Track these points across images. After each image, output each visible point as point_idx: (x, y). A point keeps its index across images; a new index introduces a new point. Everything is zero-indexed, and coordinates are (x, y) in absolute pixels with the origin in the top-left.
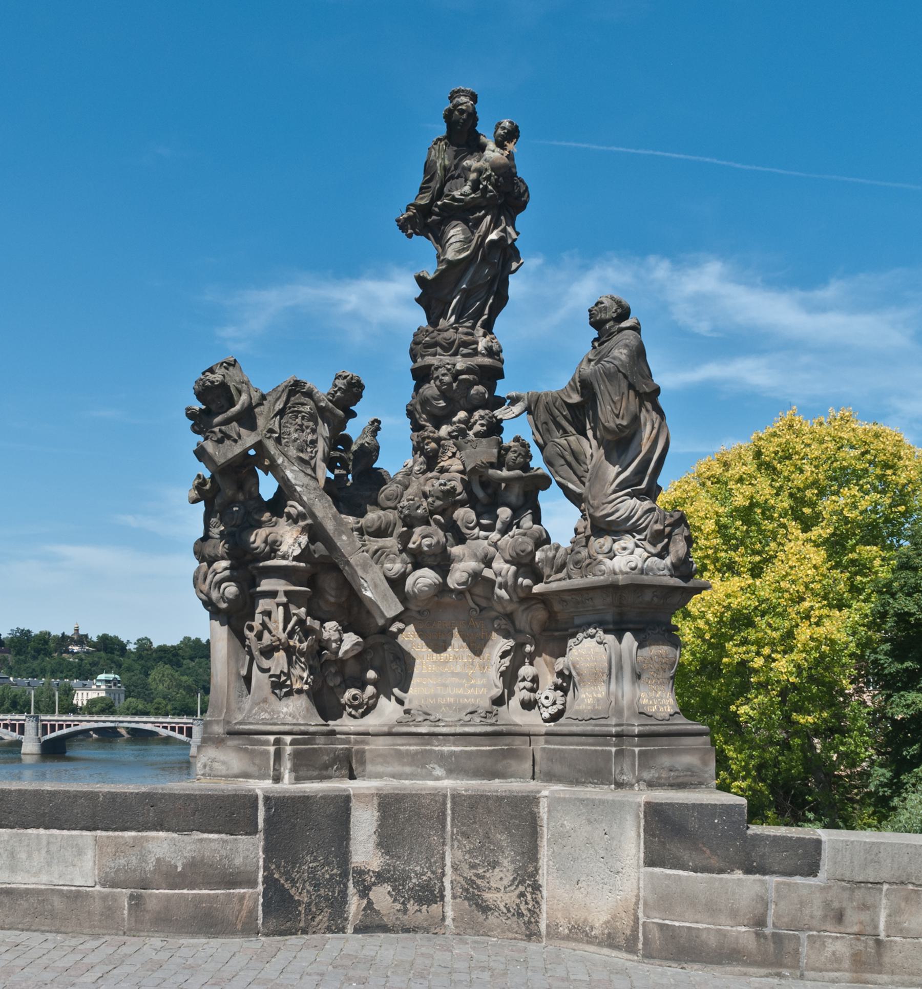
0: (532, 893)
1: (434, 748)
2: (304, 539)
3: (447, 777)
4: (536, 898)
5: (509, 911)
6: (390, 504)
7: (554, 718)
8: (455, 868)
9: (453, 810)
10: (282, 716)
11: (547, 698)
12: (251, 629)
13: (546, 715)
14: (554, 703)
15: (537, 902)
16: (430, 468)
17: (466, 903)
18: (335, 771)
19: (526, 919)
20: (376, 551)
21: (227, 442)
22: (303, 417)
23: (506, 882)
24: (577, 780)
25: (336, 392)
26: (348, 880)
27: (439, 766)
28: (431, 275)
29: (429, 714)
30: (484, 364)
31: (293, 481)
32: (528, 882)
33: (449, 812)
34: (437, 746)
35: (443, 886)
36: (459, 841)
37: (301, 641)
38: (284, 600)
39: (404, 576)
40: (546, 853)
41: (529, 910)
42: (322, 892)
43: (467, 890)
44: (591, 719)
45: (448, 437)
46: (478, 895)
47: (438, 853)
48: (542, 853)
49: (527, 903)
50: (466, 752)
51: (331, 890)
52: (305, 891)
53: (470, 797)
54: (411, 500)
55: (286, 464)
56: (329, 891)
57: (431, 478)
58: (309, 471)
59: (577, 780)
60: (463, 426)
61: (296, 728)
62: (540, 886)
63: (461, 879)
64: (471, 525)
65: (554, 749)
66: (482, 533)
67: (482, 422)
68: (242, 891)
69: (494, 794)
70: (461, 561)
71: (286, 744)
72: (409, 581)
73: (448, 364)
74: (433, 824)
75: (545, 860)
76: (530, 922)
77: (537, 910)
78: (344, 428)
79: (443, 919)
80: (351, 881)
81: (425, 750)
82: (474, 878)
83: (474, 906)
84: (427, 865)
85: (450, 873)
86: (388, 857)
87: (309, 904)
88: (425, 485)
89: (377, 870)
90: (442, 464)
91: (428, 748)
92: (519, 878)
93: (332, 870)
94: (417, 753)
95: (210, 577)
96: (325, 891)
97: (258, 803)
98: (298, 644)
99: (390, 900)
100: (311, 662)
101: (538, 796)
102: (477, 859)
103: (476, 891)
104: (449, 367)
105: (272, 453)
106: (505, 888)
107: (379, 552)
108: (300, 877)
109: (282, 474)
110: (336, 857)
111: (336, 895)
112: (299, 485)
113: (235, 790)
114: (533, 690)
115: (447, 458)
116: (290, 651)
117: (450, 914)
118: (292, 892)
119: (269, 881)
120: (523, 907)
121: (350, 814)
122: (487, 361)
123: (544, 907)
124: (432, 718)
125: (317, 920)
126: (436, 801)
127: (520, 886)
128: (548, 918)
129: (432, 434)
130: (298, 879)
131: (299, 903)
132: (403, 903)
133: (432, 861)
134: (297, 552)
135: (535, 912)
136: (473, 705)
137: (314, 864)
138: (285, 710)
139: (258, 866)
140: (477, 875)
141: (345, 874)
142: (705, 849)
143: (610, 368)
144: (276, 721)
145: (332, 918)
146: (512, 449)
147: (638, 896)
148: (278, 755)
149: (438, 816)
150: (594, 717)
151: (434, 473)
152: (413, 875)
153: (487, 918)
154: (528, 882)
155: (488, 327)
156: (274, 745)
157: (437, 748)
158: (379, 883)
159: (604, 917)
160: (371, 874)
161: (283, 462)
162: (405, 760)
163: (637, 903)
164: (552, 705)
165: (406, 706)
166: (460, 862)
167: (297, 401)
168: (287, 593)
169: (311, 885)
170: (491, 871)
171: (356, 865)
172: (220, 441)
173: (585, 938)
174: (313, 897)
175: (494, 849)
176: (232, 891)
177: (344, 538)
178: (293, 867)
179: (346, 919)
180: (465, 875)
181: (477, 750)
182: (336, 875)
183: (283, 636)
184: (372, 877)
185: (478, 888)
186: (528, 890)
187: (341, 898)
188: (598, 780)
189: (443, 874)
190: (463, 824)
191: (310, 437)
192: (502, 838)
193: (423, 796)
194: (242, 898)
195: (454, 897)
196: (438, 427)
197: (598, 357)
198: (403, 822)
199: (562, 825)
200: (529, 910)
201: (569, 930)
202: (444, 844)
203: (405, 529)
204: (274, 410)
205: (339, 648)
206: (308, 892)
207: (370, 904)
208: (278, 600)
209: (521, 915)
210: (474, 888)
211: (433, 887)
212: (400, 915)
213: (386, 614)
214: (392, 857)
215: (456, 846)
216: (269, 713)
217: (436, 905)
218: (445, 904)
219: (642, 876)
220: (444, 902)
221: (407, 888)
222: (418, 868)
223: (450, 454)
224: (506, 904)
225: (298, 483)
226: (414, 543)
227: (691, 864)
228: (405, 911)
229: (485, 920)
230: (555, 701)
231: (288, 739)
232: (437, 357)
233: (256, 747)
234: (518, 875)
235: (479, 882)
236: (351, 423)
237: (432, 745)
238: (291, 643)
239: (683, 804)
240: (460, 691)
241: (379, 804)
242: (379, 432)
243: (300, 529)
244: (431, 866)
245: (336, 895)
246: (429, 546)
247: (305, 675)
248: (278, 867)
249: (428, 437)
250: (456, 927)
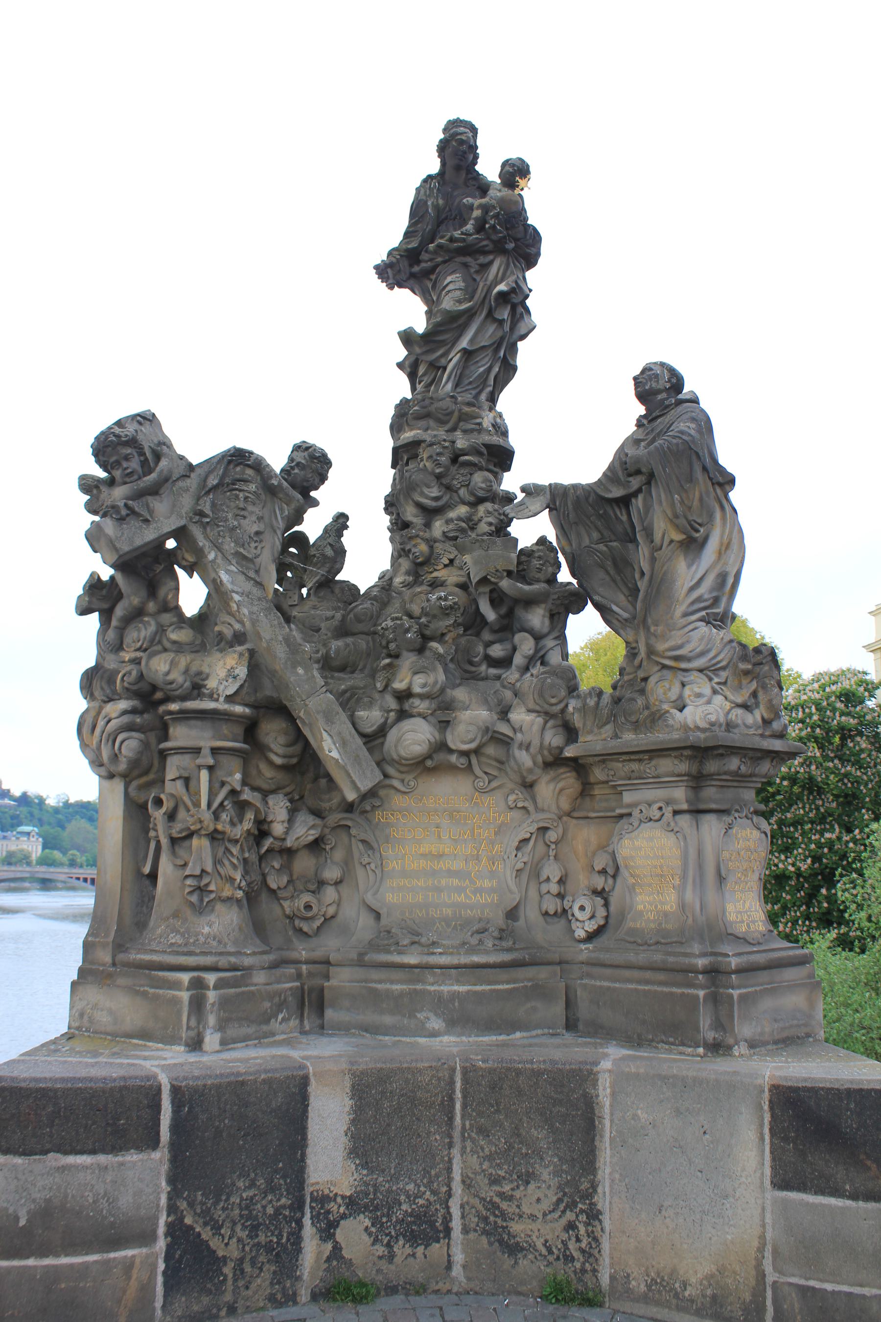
0: (587, 1224)
1: (428, 987)
2: (242, 672)
3: (447, 1032)
4: (593, 1232)
5: (550, 1252)
6: (360, 627)
7: (591, 937)
8: (467, 1183)
9: (465, 1092)
10: (202, 939)
11: (582, 908)
12: (159, 802)
13: (580, 933)
14: (592, 917)
15: (596, 1239)
16: (417, 581)
17: (484, 1238)
18: (280, 1023)
19: (578, 1265)
20: (345, 692)
21: (134, 523)
22: (246, 498)
23: (546, 1205)
24: (639, 1036)
25: (292, 468)
26: (303, 1216)
27: (436, 1014)
28: (421, 327)
29: (418, 934)
30: (493, 443)
31: (230, 586)
32: (580, 1205)
33: (458, 1095)
34: (432, 984)
35: (449, 1213)
36: (473, 1141)
37: (233, 824)
38: (211, 761)
39: (382, 731)
40: (608, 1160)
41: (583, 1251)
42: (262, 1238)
43: (485, 1219)
44: (658, 943)
45: (443, 539)
46: (502, 1227)
47: (442, 1160)
48: (602, 1160)
49: (578, 1240)
50: (476, 992)
51: (276, 1233)
52: (235, 1240)
53: (491, 1071)
54: (397, 618)
55: (219, 561)
56: (272, 1235)
57: (420, 593)
58: (252, 574)
59: (639, 1036)
60: (464, 525)
61: (223, 962)
62: (600, 1212)
63: (476, 1202)
64: (477, 659)
65: (601, 987)
66: (493, 671)
67: (490, 519)
68: (129, 1253)
69: (528, 1066)
70: (466, 709)
71: (208, 988)
72: (392, 735)
73: (445, 440)
74: (434, 1115)
75: (608, 1171)
76: (583, 1271)
77: (595, 1252)
78: (299, 520)
79: (449, 1266)
80: (308, 1215)
81: (415, 989)
82: (496, 1199)
83: (497, 1244)
84: (425, 1181)
85: (460, 1191)
86: (365, 1172)
87: (241, 1260)
88: (411, 602)
89: (348, 1194)
90: (435, 574)
91: (419, 987)
92: (566, 1199)
93: (279, 1200)
94: (402, 994)
95: (101, 723)
96: (266, 1236)
97: (160, 1100)
98: (228, 829)
99: (367, 1240)
100: (247, 855)
101: (595, 1069)
102: (501, 1169)
103: (499, 1221)
104: (447, 444)
105: (201, 544)
106: (545, 1215)
107: (348, 695)
108: (227, 1217)
109: (213, 575)
110: (284, 1177)
111: (284, 1240)
112: (237, 593)
113: (124, 1078)
114: (561, 896)
115: (442, 566)
116: (215, 836)
117: (459, 1257)
118: (215, 1243)
119: (176, 1230)
120: (572, 1245)
121: (308, 1105)
122: (496, 440)
123: (606, 1246)
124: (423, 940)
125: (253, 1286)
126: (439, 1079)
127: (568, 1213)
128: (612, 1265)
129: (421, 534)
130: (224, 1221)
132: (388, 1245)
133: (433, 1172)
134: (231, 691)
135: (591, 1255)
136: (480, 920)
137: (251, 1193)
138: (206, 930)
139: (158, 1205)
140: (501, 1195)
141: (299, 1206)
142: (869, 1163)
143: (677, 444)
144: (192, 948)
145: (277, 1278)
146: (537, 555)
147: (762, 1237)
148: (198, 1005)
149: (443, 1101)
150: (663, 941)
151: (424, 588)
152: (403, 1198)
153: (516, 1263)
154: (580, 1205)
155: (493, 399)
156: (188, 989)
157: (432, 988)
158: (350, 1215)
159: (706, 1268)
160: (339, 1200)
161: (215, 558)
162: (384, 1005)
163: (761, 1249)
164: (590, 919)
165: (384, 921)
166: (475, 1173)
167: (238, 476)
168: (215, 751)
169: (244, 1227)
170: (522, 1188)
171: (317, 1187)
172: (121, 519)
173: (674, 1301)
174: (247, 1248)
175: (527, 1154)
176: (112, 1255)
177: (300, 671)
178: (216, 1203)
179: (299, 1278)
180: (483, 1195)
181: (490, 990)
182: (284, 1207)
183: (207, 816)
184: (340, 1206)
185: (503, 1215)
186: (580, 1218)
187: (292, 1244)
188: (676, 1039)
189: (449, 1194)
190: (480, 1114)
191: (255, 528)
192: (540, 1135)
193: (420, 1071)
194: (128, 1266)
195: (465, 1230)
196: (428, 525)
197: (651, 437)
198: (388, 1114)
199: (635, 1117)
200: (583, 1251)
201: (647, 1285)
202: (450, 1145)
203: (387, 661)
204: (204, 486)
205: (287, 833)
206: (239, 1240)
207: (337, 1248)
208: (199, 761)
209: (569, 1259)
210: (496, 1216)
211: (433, 1215)
212: (384, 1265)
213: (359, 784)
214: (371, 1171)
215: (468, 1149)
216: (183, 935)
217: (437, 1245)
218: (452, 1242)
219: (768, 1203)
220: (449, 1239)
221: (394, 1219)
222: (411, 1187)
223: (447, 562)
224: (546, 1241)
225: (235, 589)
226: (402, 681)
227: (848, 1187)
228: (391, 1257)
229: (513, 1267)
230: (594, 913)
231: (211, 978)
232: (429, 432)
233: (161, 991)
234: (565, 1194)
235: (504, 1205)
236: (310, 515)
237: (424, 982)
238: (220, 827)
239: (832, 1089)
240: (462, 898)
241: (353, 1086)
242: (345, 532)
243: (236, 656)
244: (431, 1182)
245: (284, 1240)
246: (424, 686)
247: (238, 877)
248: (191, 1205)
249: (417, 536)
250: (469, 1279)
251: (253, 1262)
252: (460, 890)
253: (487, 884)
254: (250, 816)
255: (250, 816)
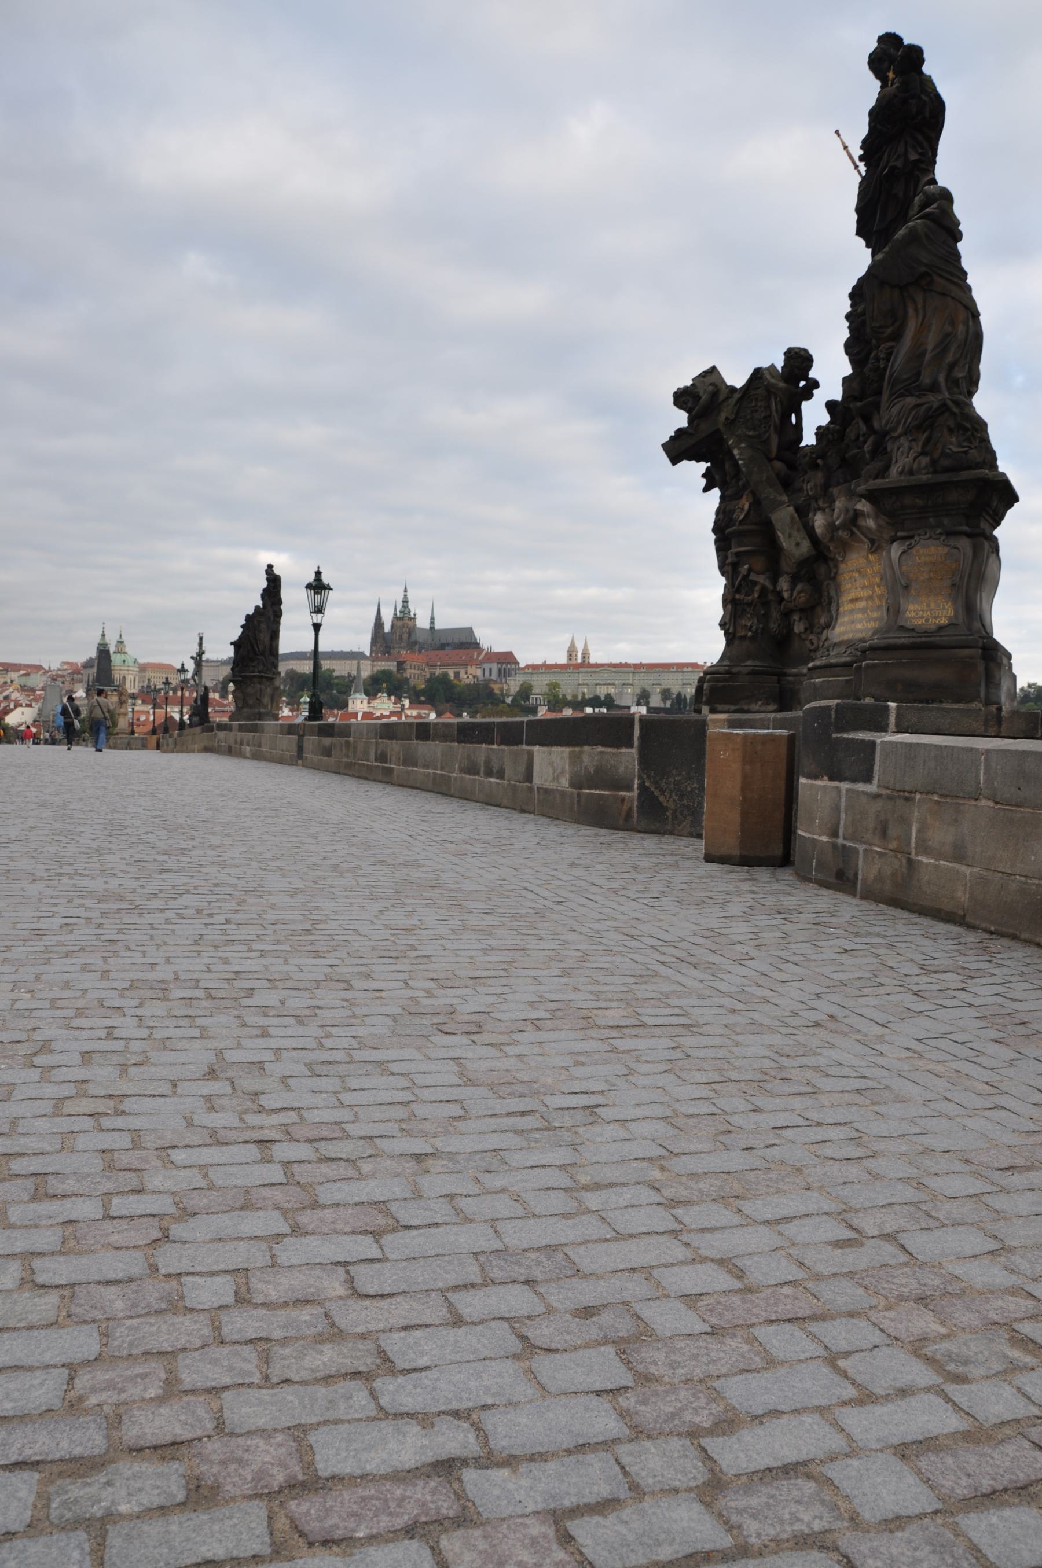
118: (661, 799)
119: (642, 787)
131: (667, 809)
191: (763, 415)
194: (623, 800)
205: (792, 595)
206: (674, 800)
238: (737, 596)
240: (860, 626)
251: (682, 814)
252: (861, 621)
253: (875, 615)
254: (757, 588)
255: (757, 588)
